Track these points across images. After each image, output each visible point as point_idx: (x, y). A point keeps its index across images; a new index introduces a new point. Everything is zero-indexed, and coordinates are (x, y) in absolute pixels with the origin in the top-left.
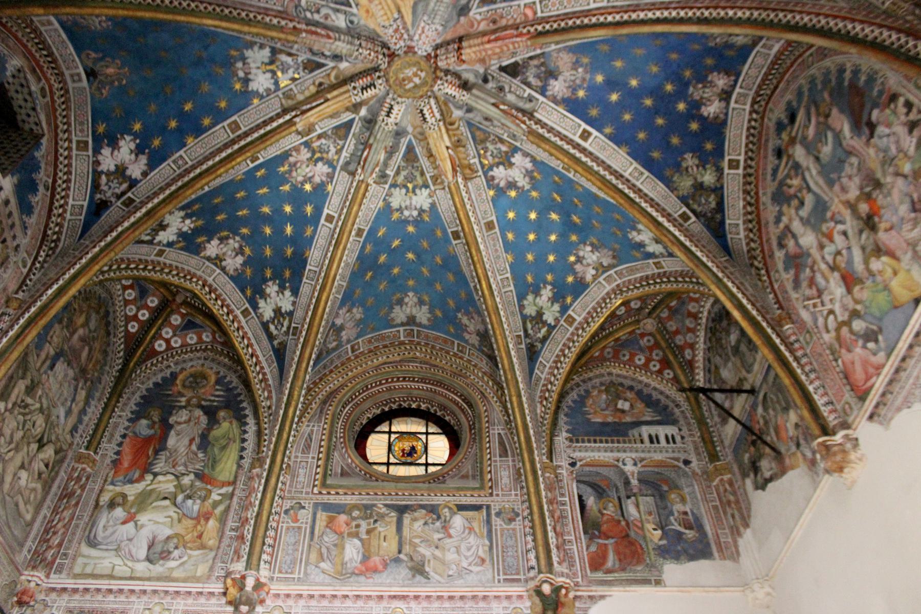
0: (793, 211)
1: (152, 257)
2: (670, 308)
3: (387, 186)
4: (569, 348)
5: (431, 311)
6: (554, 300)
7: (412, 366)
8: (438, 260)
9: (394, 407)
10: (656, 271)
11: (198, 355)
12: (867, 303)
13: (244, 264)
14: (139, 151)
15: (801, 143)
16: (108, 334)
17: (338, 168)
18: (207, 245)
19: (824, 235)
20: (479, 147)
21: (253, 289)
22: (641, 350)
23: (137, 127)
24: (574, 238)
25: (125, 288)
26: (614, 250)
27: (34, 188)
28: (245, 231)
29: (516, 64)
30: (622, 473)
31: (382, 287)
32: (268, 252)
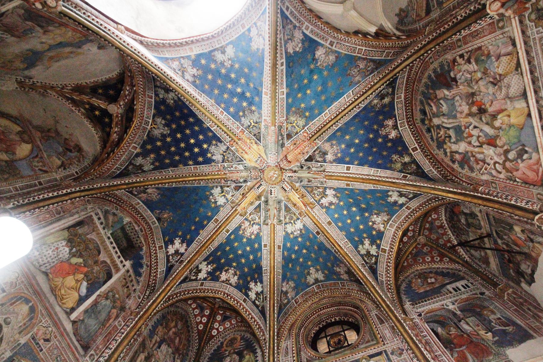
0: (449, 144)
1: (199, 287)
2: (427, 229)
3: (283, 225)
4: (389, 262)
5: (323, 273)
6: (372, 244)
7: (324, 301)
8: (316, 247)
9: (324, 324)
10: (409, 211)
11: (232, 331)
12: (508, 142)
13: (238, 279)
14: (182, 242)
15: (434, 117)
16: (189, 331)
19: (467, 138)
21: (243, 288)
22: (426, 254)
23: (180, 234)
24: (367, 214)
25: (194, 309)
26: (386, 211)
27: (141, 266)
28: (234, 264)
29: (310, 156)
30: (449, 311)
31: (298, 269)
32: (246, 270)
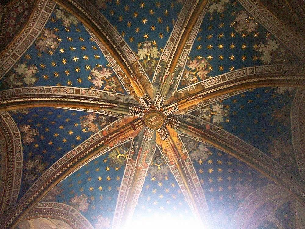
3: (160, 59)
6: (61, 21)
17: (184, 68)
18: (253, 30)
20: (119, 84)
